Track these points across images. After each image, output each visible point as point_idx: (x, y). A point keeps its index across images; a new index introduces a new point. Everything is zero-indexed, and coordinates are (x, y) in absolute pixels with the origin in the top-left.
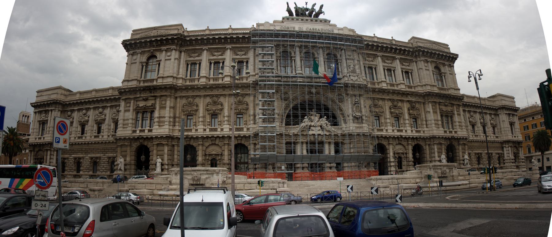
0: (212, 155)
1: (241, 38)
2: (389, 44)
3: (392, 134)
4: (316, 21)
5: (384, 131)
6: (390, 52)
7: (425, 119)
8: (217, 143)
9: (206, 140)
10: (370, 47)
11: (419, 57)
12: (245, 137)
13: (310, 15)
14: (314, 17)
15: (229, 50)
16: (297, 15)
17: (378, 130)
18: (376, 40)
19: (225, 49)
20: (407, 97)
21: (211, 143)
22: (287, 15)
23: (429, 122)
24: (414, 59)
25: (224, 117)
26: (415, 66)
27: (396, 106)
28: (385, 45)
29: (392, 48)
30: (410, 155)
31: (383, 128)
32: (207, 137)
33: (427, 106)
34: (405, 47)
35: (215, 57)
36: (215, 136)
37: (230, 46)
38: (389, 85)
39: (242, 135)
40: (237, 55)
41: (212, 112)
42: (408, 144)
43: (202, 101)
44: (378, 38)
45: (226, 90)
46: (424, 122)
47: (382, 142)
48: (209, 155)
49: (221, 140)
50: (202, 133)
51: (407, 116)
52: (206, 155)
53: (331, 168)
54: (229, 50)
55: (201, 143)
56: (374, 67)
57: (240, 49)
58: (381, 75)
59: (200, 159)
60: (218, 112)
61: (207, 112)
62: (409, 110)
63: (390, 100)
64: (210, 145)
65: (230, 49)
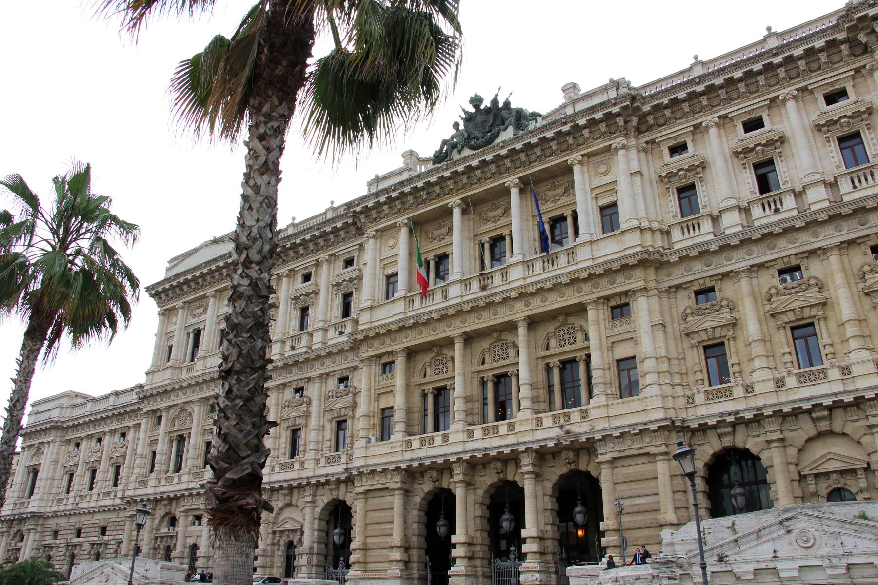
0: (827, 474)
8: (837, 427)
9: (790, 424)
21: (812, 432)
25: (842, 325)
32: (797, 413)
36: (827, 402)
41: (791, 317)
48: (817, 476)
49: (853, 414)
50: (772, 400)
52: (802, 478)
55: (778, 436)
60: (814, 312)
61: (772, 323)
64: (809, 440)
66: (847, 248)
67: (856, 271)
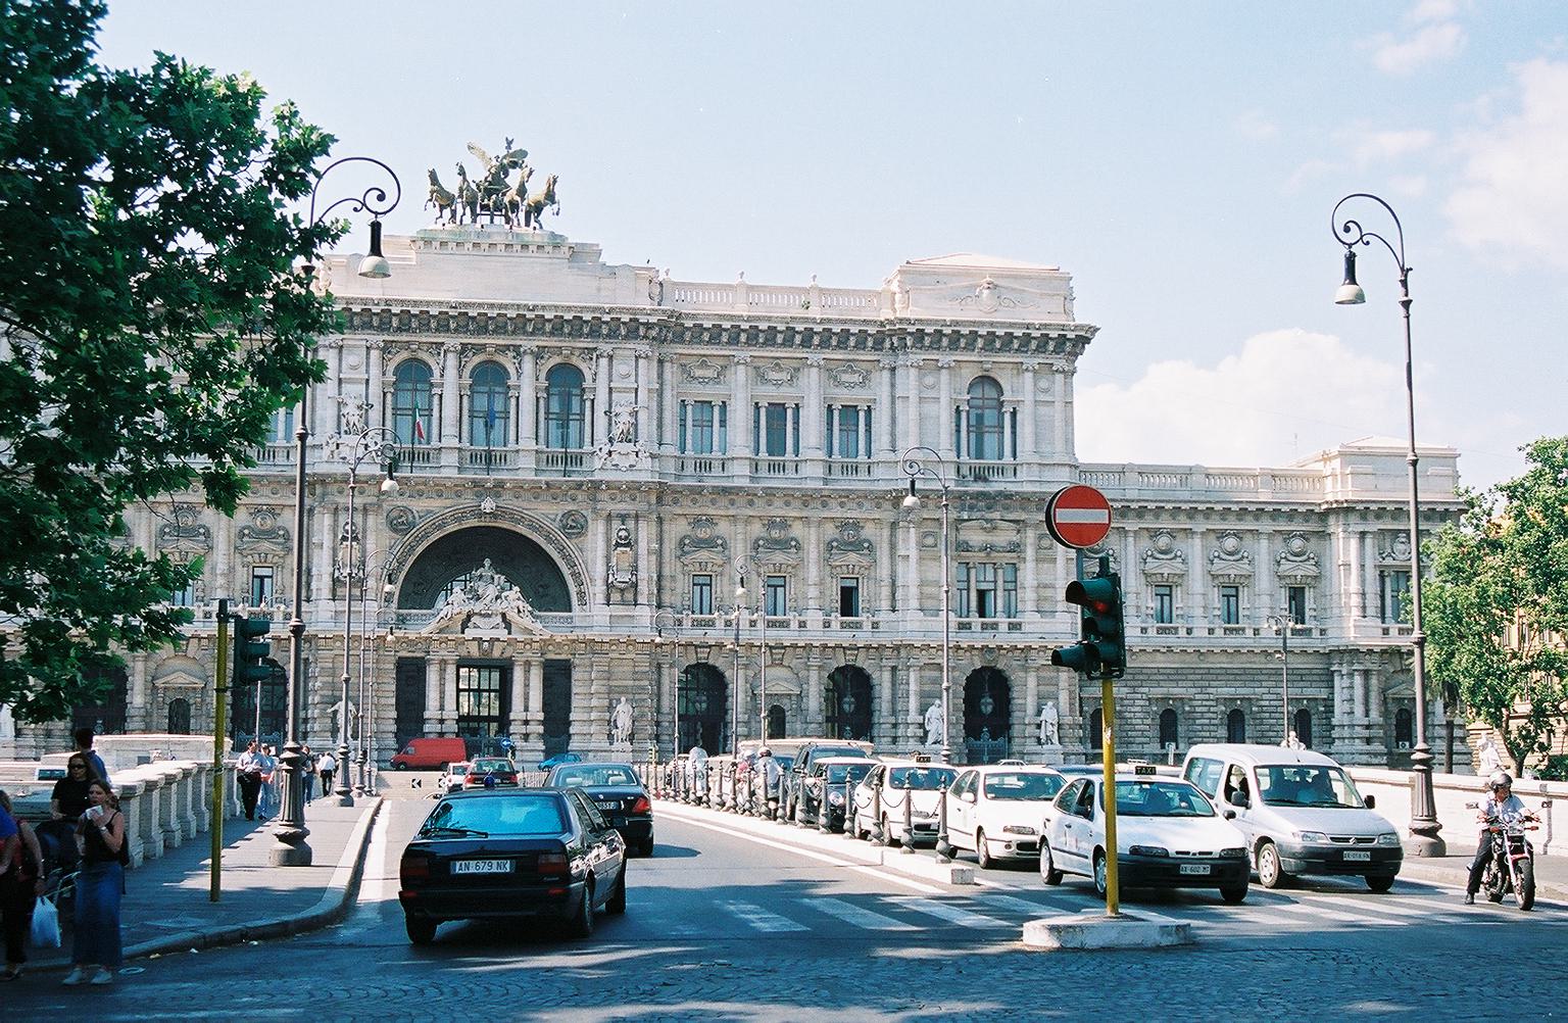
2: (782, 320)
4: (525, 247)
6: (788, 342)
7: (887, 581)
11: (906, 354)
20: (824, 505)
23: (898, 596)
24: (886, 361)
26: (886, 389)
27: (776, 542)
30: (814, 702)
33: (900, 534)
34: (845, 322)
42: (808, 668)
43: (144, 522)
46: (886, 591)
51: (813, 572)
53: (526, 737)
56: (717, 402)
58: (739, 436)
59: (137, 699)
62: (829, 547)
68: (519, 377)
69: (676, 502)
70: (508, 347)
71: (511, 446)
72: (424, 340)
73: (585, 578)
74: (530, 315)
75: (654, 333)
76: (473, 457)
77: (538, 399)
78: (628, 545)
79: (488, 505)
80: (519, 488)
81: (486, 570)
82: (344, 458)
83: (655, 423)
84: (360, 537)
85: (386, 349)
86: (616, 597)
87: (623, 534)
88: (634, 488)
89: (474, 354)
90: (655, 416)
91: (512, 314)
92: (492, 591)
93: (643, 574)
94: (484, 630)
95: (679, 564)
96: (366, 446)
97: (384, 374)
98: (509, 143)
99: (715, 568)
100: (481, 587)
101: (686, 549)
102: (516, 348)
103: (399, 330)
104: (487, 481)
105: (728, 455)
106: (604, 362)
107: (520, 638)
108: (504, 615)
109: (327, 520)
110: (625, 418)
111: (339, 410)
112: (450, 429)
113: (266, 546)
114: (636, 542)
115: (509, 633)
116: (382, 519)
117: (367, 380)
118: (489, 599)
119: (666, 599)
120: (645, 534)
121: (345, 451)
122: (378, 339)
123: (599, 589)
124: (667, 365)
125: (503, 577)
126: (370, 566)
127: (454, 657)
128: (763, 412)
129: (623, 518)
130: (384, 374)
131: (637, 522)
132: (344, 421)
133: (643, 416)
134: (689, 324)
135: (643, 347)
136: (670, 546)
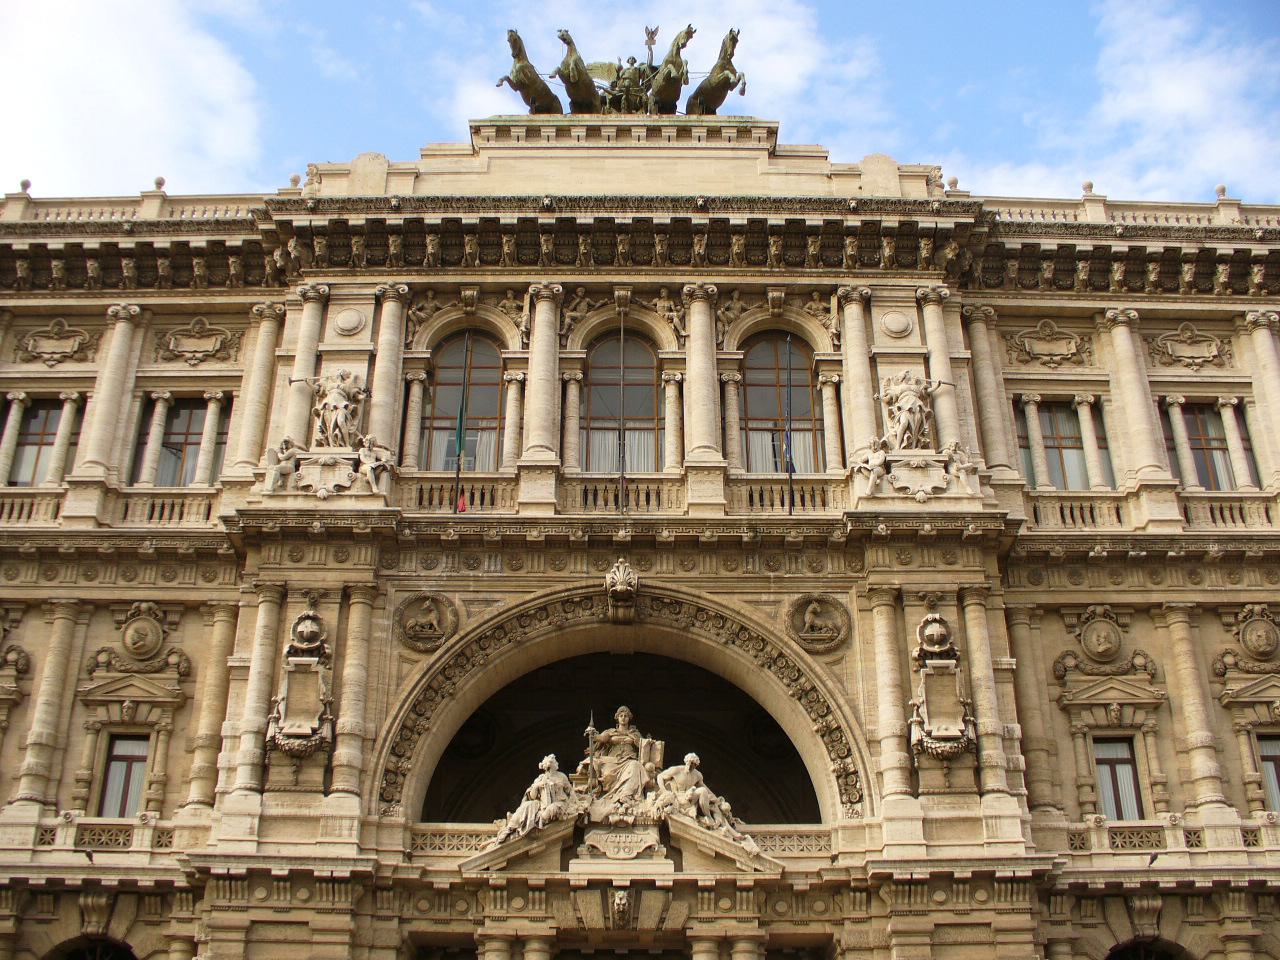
1: (199, 252)
2: (1190, 234)
3: (1241, 861)
5: (1175, 841)
6: (1203, 284)
10: (1047, 270)
12: (128, 889)
13: (666, 106)
14: (690, 110)
15: (120, 329)
16: (579, 106)
17: (1123, 838)
18: (1093, 215)
19: (99, 320)
22: (514, 107)
25: (23, 749)
28: (1155, 246)
29: (1207, 261)
31: (1162, 819)
35: (36, 369)
37: (132, 303)
38: (1201, 512)
39: (111, 880)
40: (176, 357)
44: (1110, 207)
45: (66, 574)
47: (1168, 933)
54: (120, 329)
57: (198, 320)
63: (1213, 611)
65: (131, 319)
66: (92, 615)
67: (86, 662)
68: (682, 346)
69: (1036, 580)
70: (654, 291)
71: (671, 468)
72: (490, 279)
73: (854, 738)
74: (698, 219)
75: (949, 253)
76: (591, 491)
77: (723, 385)
78: (948, 654)
79: (619, 575)
80: (690, 545)
81: (621, 732)
82: (307, 487)
83: (972, 421)
84: (329, 649)
85: (411, 298)
86: (931, 778)
87: (934, 630)
88: (946, 538)
89: (590, 307)
90: (970, 408)
91: (662, 218)
92: (631, 773)
93: (987, 722)
94: (617, 861)
95: (1060, 719)
96: (357, 464)
97: (408, 346)
98: (651, 35)
99: (1140, 717)
100: (607, 763)
101: (1070, 677)
102: (675, 293)
103: (443, 262)
104: (615, 524)
105: (1126, 485)
106: (853, 311)
107: (706, 876)
108: (663, 827)
109: (260, 617)
110: (909, 400)
111: (312, 404)
112: (537, 433)
113: (140, 687)
114: (966, 652)
115: (679, 868)
116: (384, 621)
117: (372, 357)
118: (626, 790)
119: (1044, 790)
120: (979, 634)
121: (311, 475)
122: (403, 281)
123: (890, 756)
124: (980, 328)
125: (659, 744)
126: (347, 720)
127: (545, 929)
128: (1176, 415)
129: (933, 601)
130: (408, 346)
131: (962, 609)
132: (318, 423)
133: (945, 407)
134: (1014, 243)
135: (930, 284)
136: (1036, 677)
